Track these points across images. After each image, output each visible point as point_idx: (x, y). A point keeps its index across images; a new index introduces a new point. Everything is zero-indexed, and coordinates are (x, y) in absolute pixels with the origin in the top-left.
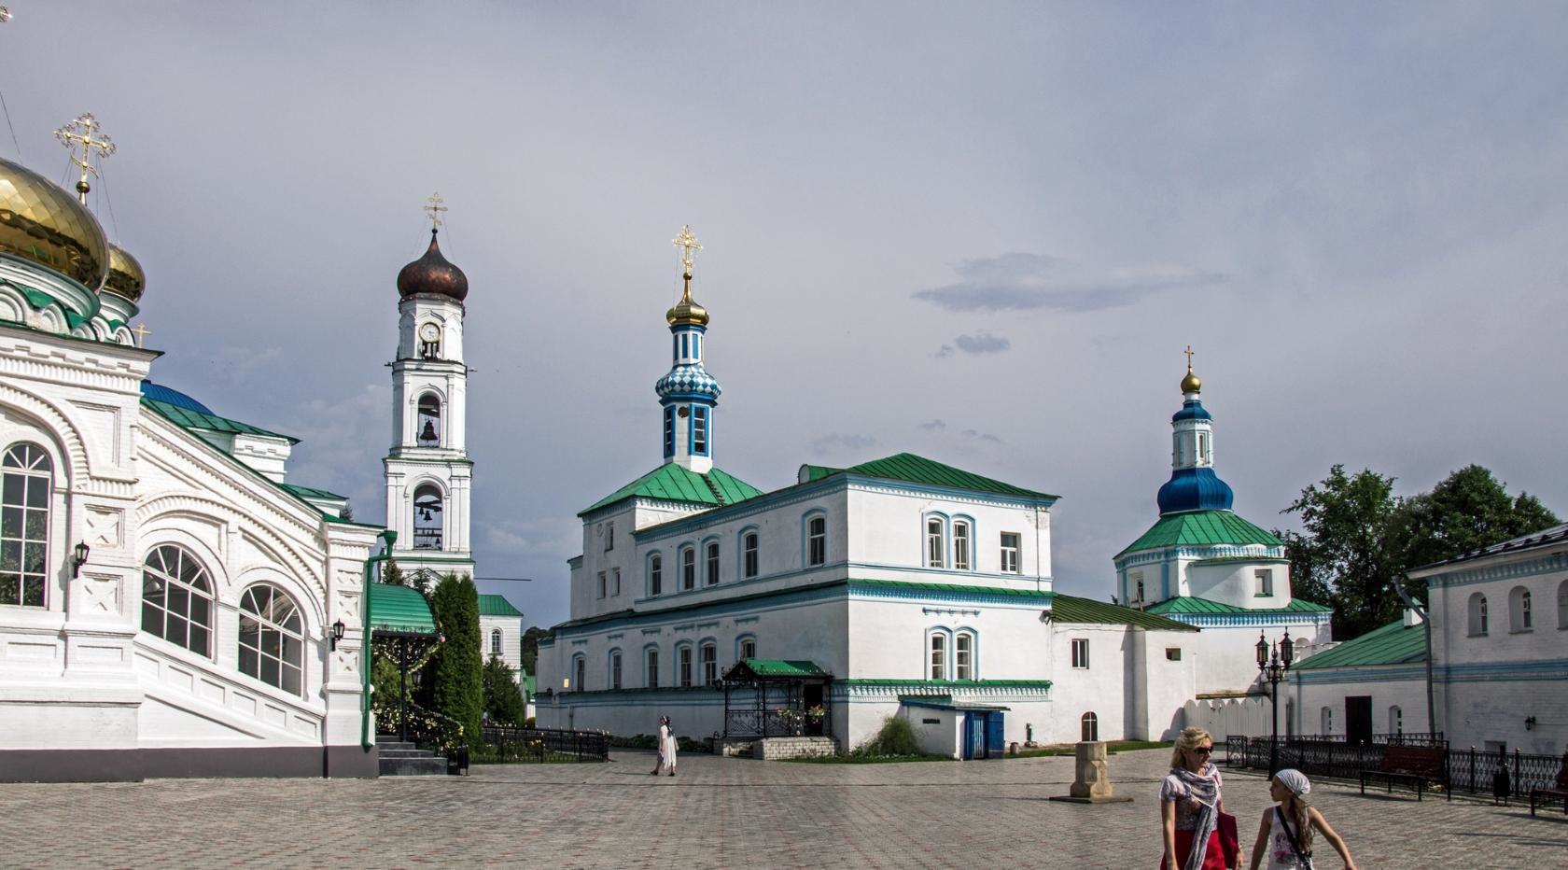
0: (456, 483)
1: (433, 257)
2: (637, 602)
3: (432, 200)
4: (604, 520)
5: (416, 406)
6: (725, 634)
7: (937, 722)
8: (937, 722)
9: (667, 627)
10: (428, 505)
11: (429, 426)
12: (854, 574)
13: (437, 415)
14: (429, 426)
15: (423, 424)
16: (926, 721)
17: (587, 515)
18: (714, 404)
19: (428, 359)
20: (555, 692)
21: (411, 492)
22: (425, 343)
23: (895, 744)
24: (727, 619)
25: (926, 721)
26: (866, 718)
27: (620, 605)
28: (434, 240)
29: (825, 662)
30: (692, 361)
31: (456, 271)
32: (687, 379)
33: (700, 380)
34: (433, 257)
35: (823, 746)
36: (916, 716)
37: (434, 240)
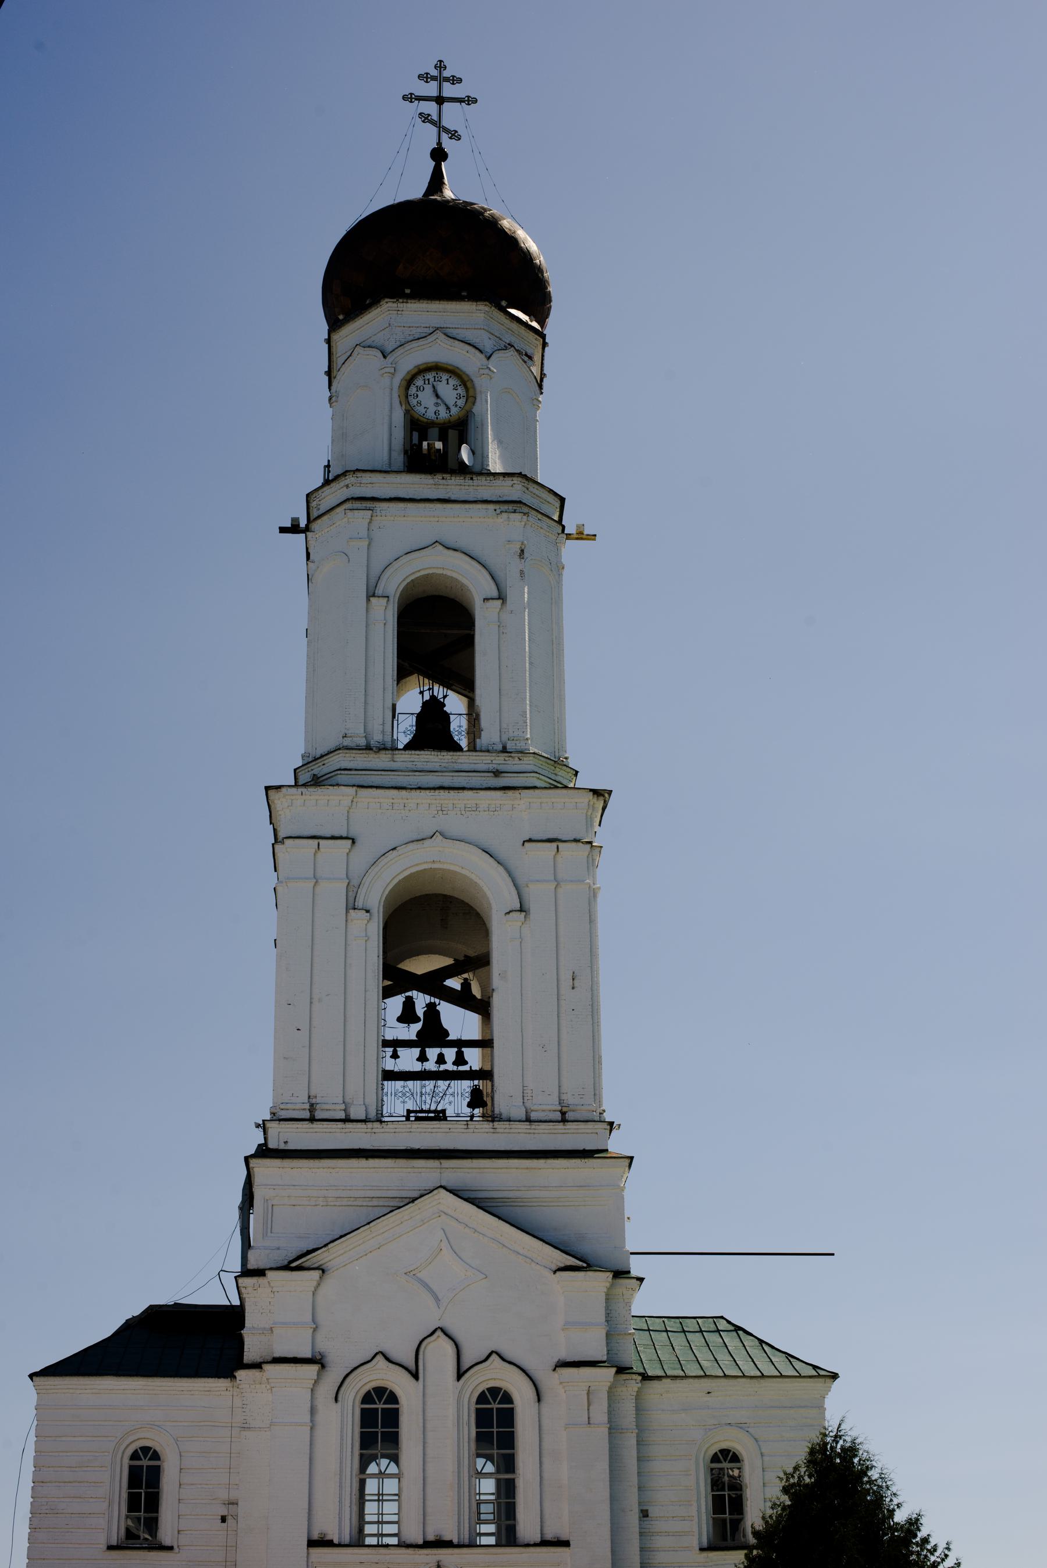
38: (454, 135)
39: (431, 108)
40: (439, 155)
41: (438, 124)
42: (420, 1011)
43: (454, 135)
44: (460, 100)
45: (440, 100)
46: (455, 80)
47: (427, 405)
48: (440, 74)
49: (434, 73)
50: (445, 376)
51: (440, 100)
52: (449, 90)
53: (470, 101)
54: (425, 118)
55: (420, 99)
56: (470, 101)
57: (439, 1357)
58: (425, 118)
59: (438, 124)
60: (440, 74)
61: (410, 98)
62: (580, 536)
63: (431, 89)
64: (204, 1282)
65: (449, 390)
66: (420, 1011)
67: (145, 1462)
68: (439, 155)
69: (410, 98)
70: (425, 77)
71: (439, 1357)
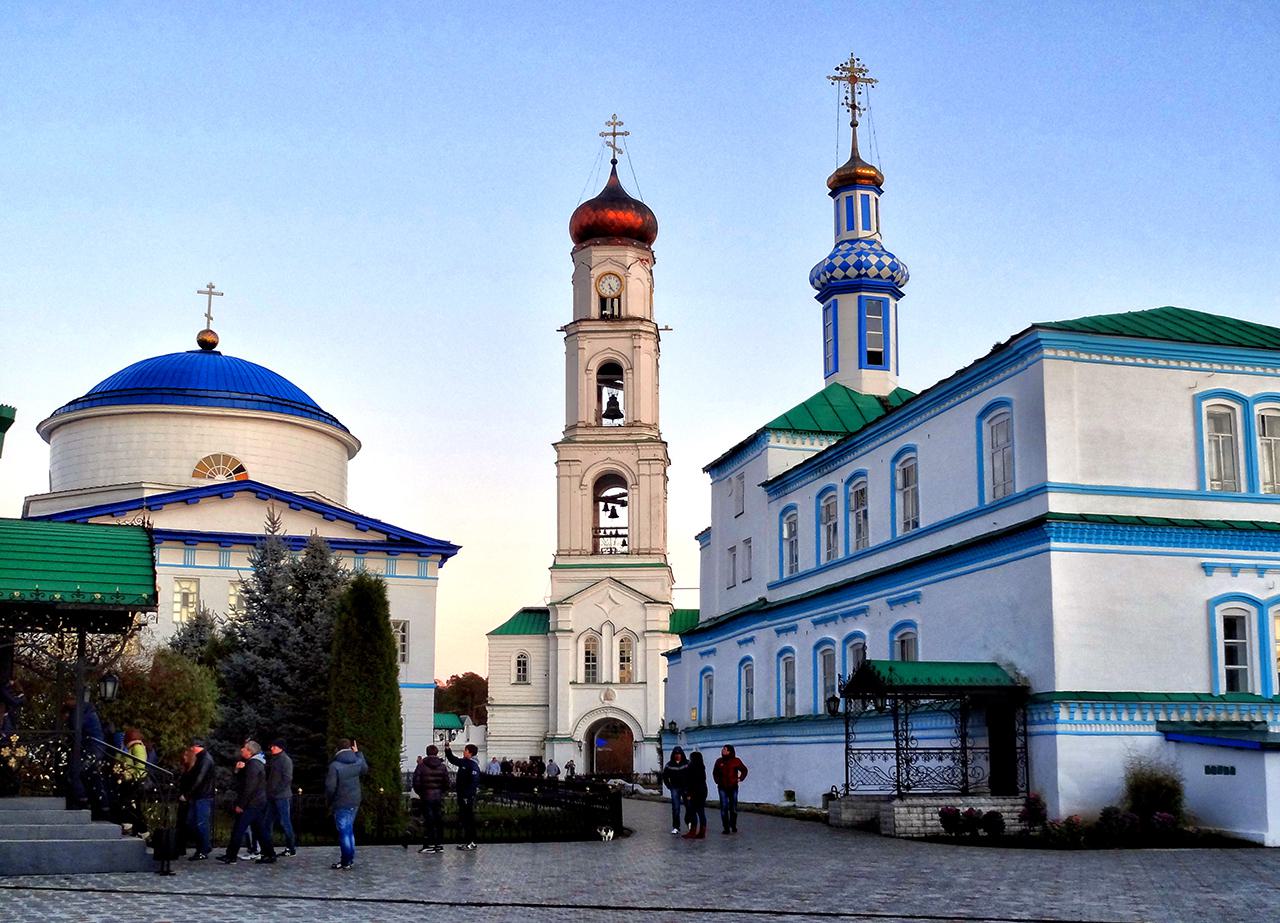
0: (644, 469)
1: (614, 195)
2: (772, 587)
3: (608, 124)
4: (732, 471)
5: (594, 376)
6: (873, 630)
7: (1231, 771)
8: (1231, 771)
9: (804, 622)
10: (613, 499)
11: (613, 400)
12: (1058, 503)
13: (620, 387)
14: (613, 400)
15: (606, 399)
16: (1210, 770)
17: (714, 468)
18: (899, 295)
19: (603, 318)
20: (680, 727)
21: (589, 481)
22: (603, 301)
23: (1148, 816)
24: (877, 602)
25: (1210, 770)
26: (1083, 764)
27: (747, 596)
28: (614, 172)
29: (1026, 667)
30: (862, 233)
31: (640, 207)
32: (852, 260)
33: (873, 259)
34: (614, 195)
35: (1009, 810)
36: (1190, 766)
37: (614, 172)
38: (620, 152)
39: (610, 139)
40: (614, 162)
41: (614, 147)
42: (610, 508)
43: (620, 152)
44: (623, 134)
45: (614, 134)
46: (621, 124)
47: (606, 292)
48: (615, 122)
49: (612, 121)
50: (613, 277)
51: (614, 134)
52: (619, 129)
53: (626, 134)
54: (609, 144)
55: (607, 134)
56: (626, 134)
57: (606, 630)
58: (609, 144)
59: (614, 147)
60: (615, 122)
61: (603, 135)
62: (667, 329)
63: (610, 129)
64: (540, 602)
65: (614, 282)
66: (610, 508)
67: (522, 659)
68: (614, 162)
69: (603, 135)
70: (608, 124)
71: (606, 630)
